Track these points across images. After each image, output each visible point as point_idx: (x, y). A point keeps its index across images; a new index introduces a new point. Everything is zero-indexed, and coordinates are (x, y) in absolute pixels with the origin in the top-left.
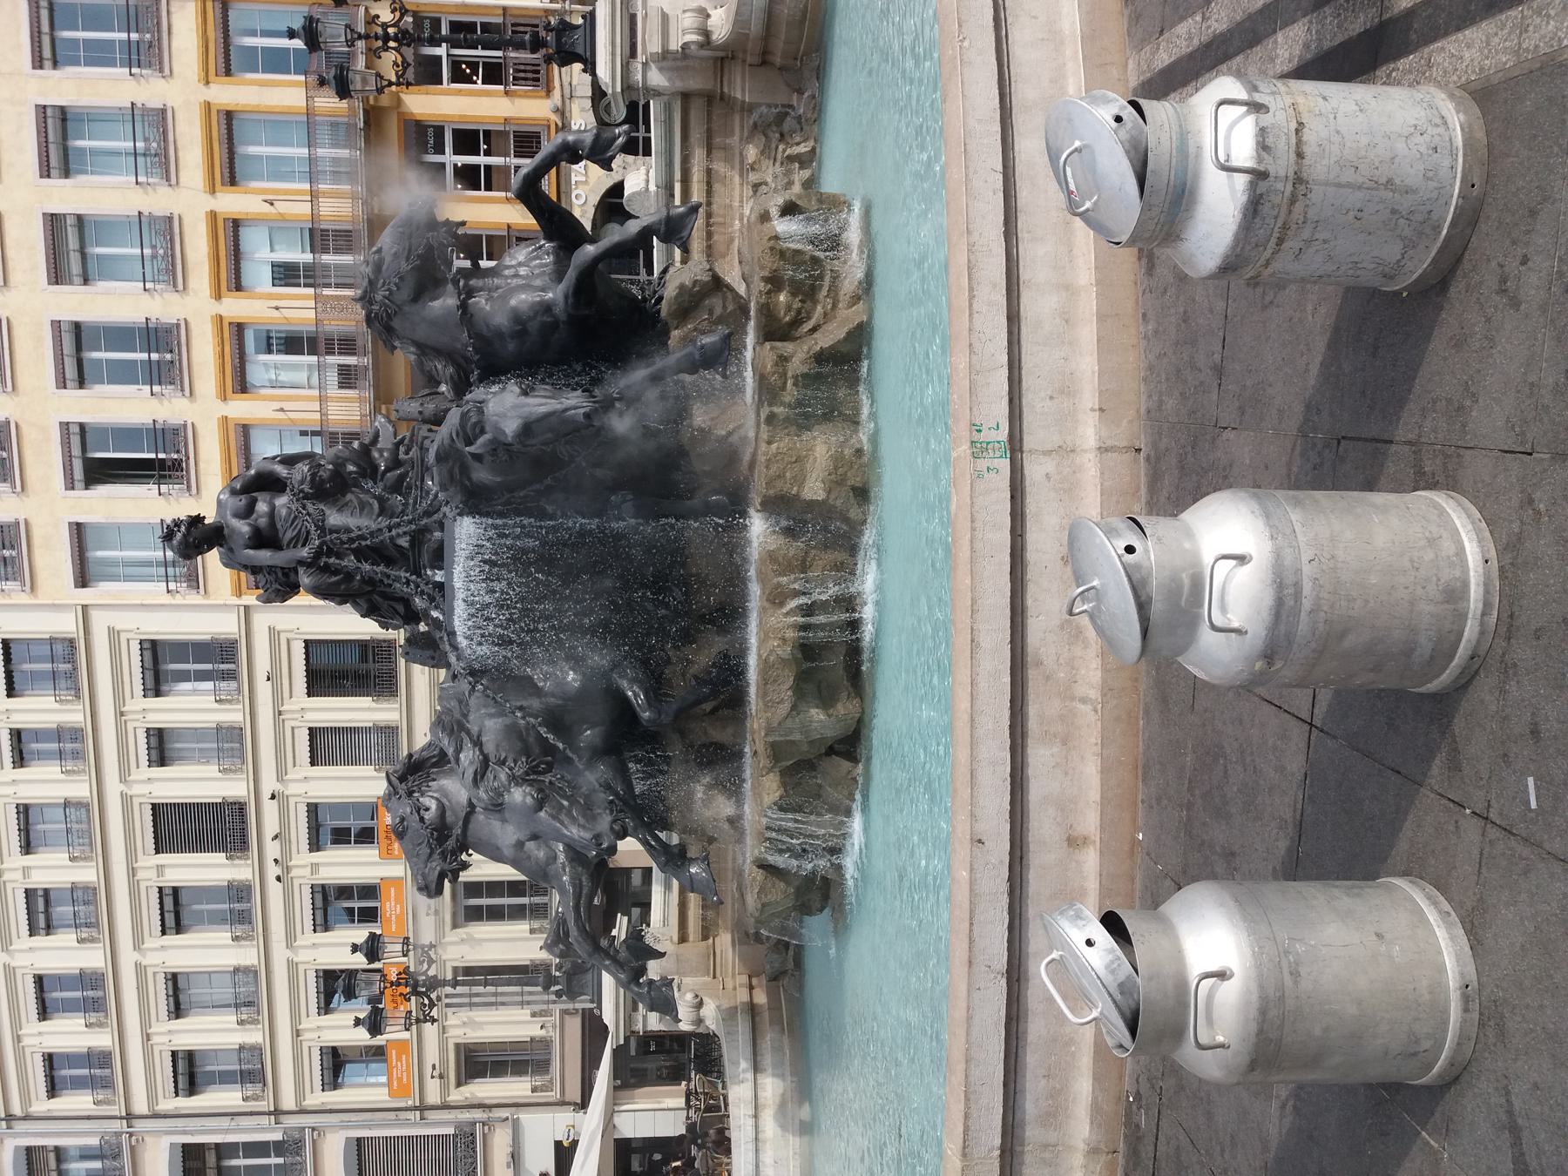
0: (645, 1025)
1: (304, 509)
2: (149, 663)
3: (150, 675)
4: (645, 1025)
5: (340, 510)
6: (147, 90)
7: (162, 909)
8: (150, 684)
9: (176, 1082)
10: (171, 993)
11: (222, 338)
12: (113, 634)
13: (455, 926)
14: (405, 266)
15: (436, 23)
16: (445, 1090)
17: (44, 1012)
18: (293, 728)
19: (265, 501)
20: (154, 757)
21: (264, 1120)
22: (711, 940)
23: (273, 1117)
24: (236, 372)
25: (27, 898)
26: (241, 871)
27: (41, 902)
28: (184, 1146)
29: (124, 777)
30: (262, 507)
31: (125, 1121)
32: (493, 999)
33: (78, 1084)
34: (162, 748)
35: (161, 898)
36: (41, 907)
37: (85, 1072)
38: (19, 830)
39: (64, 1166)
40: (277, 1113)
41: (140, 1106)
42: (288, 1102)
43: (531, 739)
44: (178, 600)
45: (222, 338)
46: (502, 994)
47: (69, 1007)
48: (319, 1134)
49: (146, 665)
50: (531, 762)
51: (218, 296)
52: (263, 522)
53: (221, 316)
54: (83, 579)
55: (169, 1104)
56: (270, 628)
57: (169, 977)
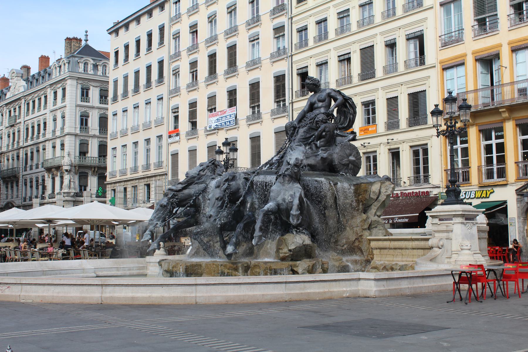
1: (310, 120)
5: (304, 132)
6: (468, 33)
7: (345, 55)
8: (410, 36)
9: (300, 69)
10: (323, 62)
13: (389, 150)
15: (502, 137)
17: (318, 23)
19: (322, 105)
20: (388, 42)
22: (479, 252)
24: (519, 47)
25: (347, 9)
26: (356, 79)
27: (346, 14)
29: (382, 33)
30: (320, 104)
34: (391, 46)
35: (348, 54)
36: (345, 15)
37: (304, 39)
38: (366, 2)
39: (281, 38)
40: (292, 103)
41: (295, 58)
43: (187, 201)
47: (320, 31)
48: (287, 117)
49: (391, 41)
50: (176, 203)
52: (316, 105)
54: (442, 5)
56: (429, 76)
57: (327, 61)
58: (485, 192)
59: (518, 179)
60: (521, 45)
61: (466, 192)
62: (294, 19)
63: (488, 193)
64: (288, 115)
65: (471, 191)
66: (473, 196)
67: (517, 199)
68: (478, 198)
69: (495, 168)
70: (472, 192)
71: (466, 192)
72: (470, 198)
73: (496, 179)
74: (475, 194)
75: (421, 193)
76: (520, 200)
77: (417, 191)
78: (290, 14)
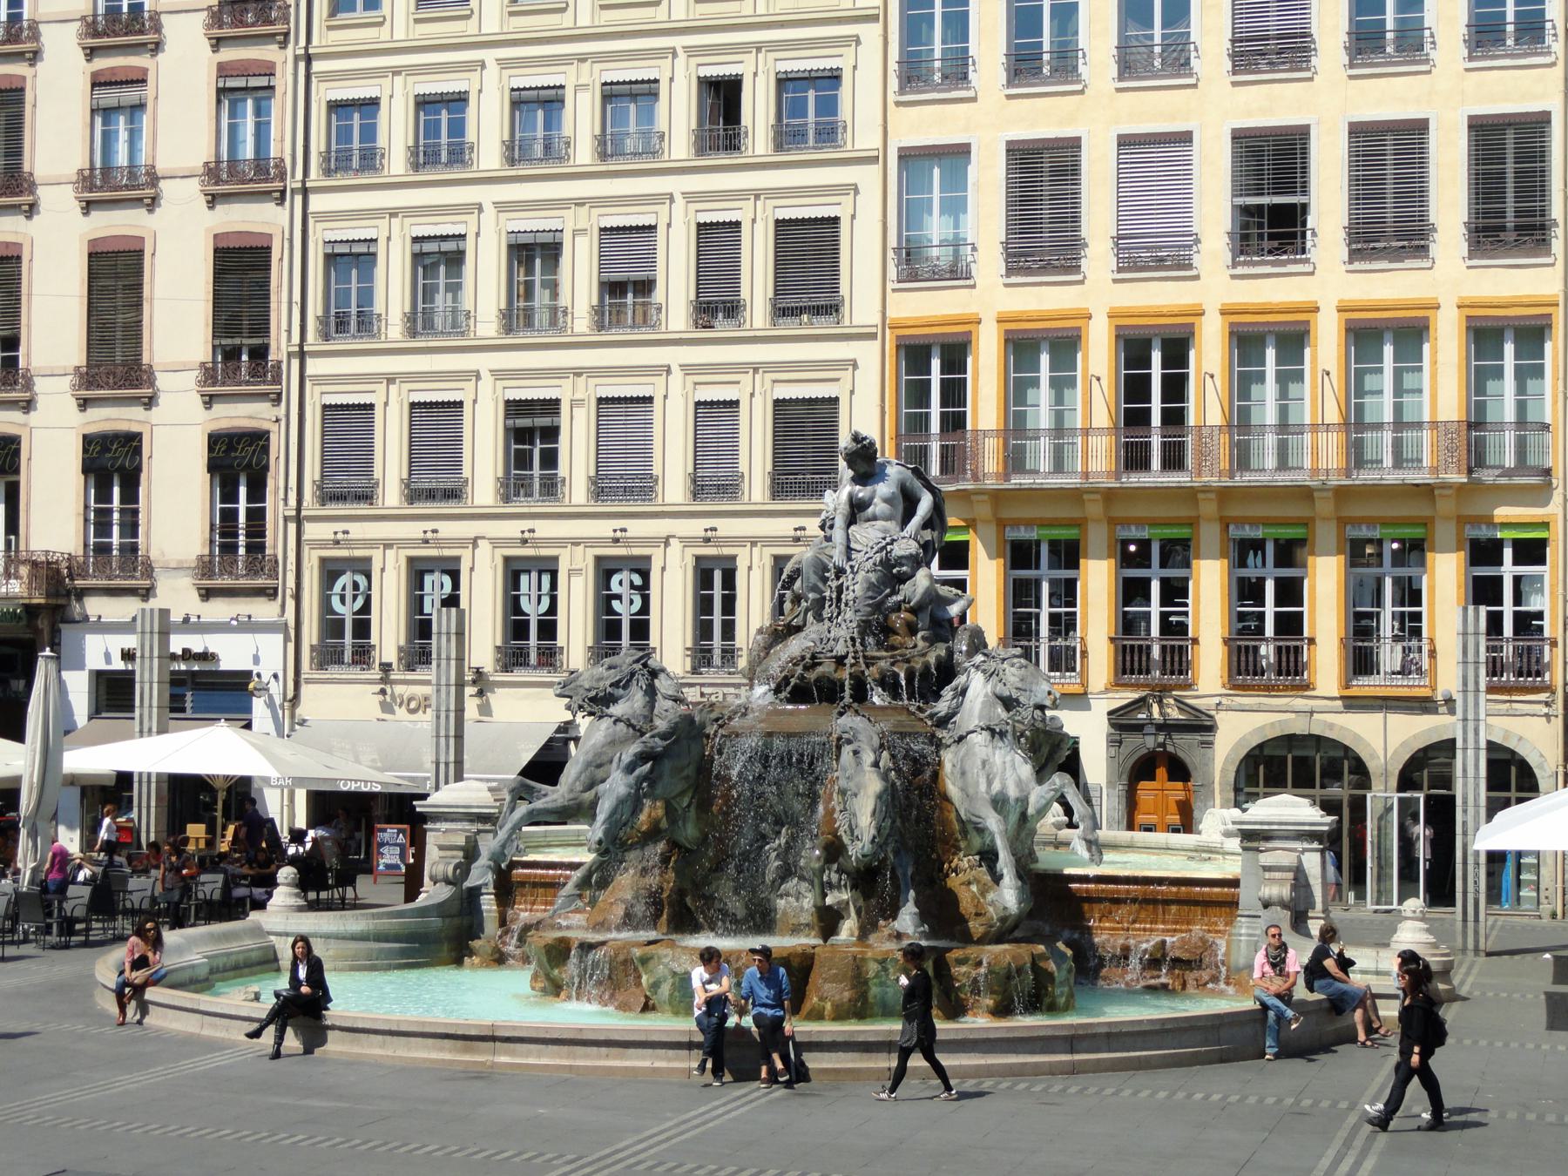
0: (432, 830)
4: (432, 830)
11: (1176, 315)
16: (320, 544)
21: (296, 339)
23: (297, 349)
28: (269, 248)
31: (299, 185)
32: (444, 656)
33: (345, 135)
40: (302, 355)
41: (317, 203)
42: (314, 367)
45: (1176, 315)
46: (448, 665)
47: (432, 130)
51: (1223, 312)
53: (1202, 314)
55: (320, 234)
62: (317, 66)
64: (280, 394)
67: (1109, 735)
78: (302, 43)
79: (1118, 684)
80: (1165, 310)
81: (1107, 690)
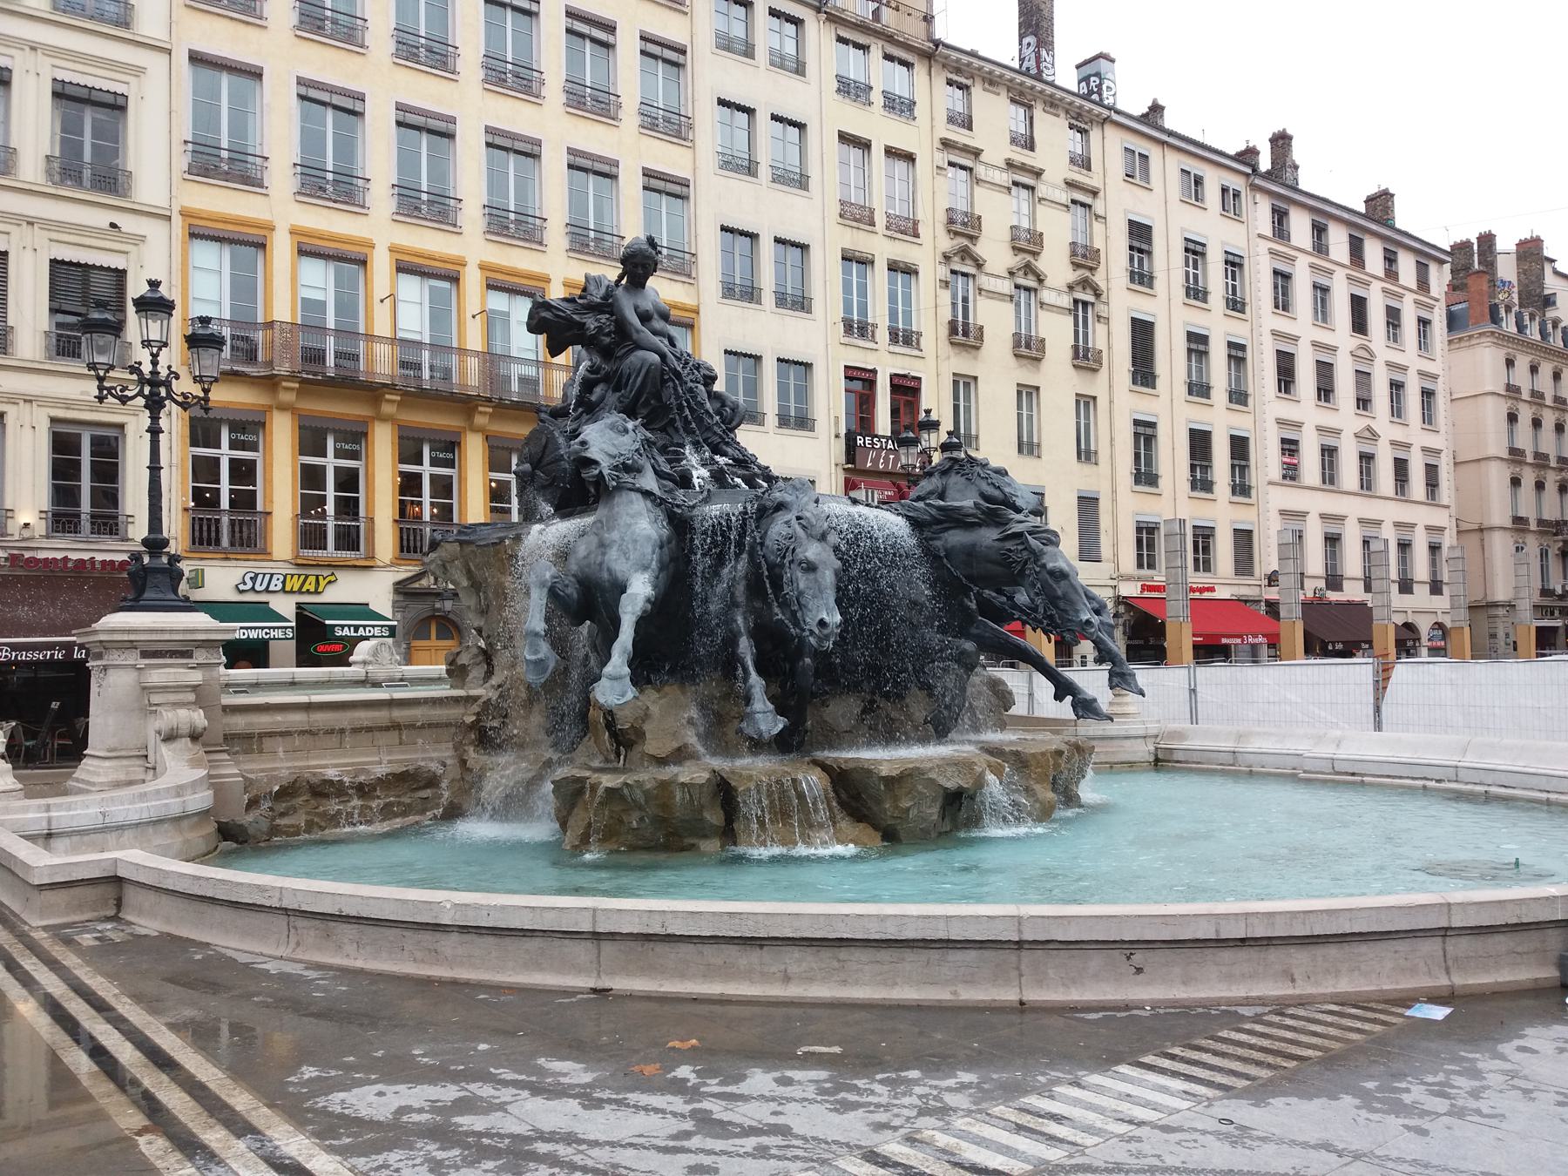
2: (95, 96)
3: (83, 93)
8: (69, 90)
12: (139, 71)
14: (1007, 490)
18: (8, 233)
44: (178, 148)
58: (312, 579)
59: (396, 562)
60: (421, 266)
61: (257, 575)
63: (322, 583)
65: (272, 575)
66: (276, 584)
67: (394, 602)
68: (292, 592)
69: (331, 525)
70: (275, 577)
71: (257, 575)
72: (253, 588)
73: (331, 551)
74: (284, 582)
75: (98, 566)
76: (404, 604)
77: (86, 556)
79: (396, 562)
80: (437, 256)
81: (392, 564)
